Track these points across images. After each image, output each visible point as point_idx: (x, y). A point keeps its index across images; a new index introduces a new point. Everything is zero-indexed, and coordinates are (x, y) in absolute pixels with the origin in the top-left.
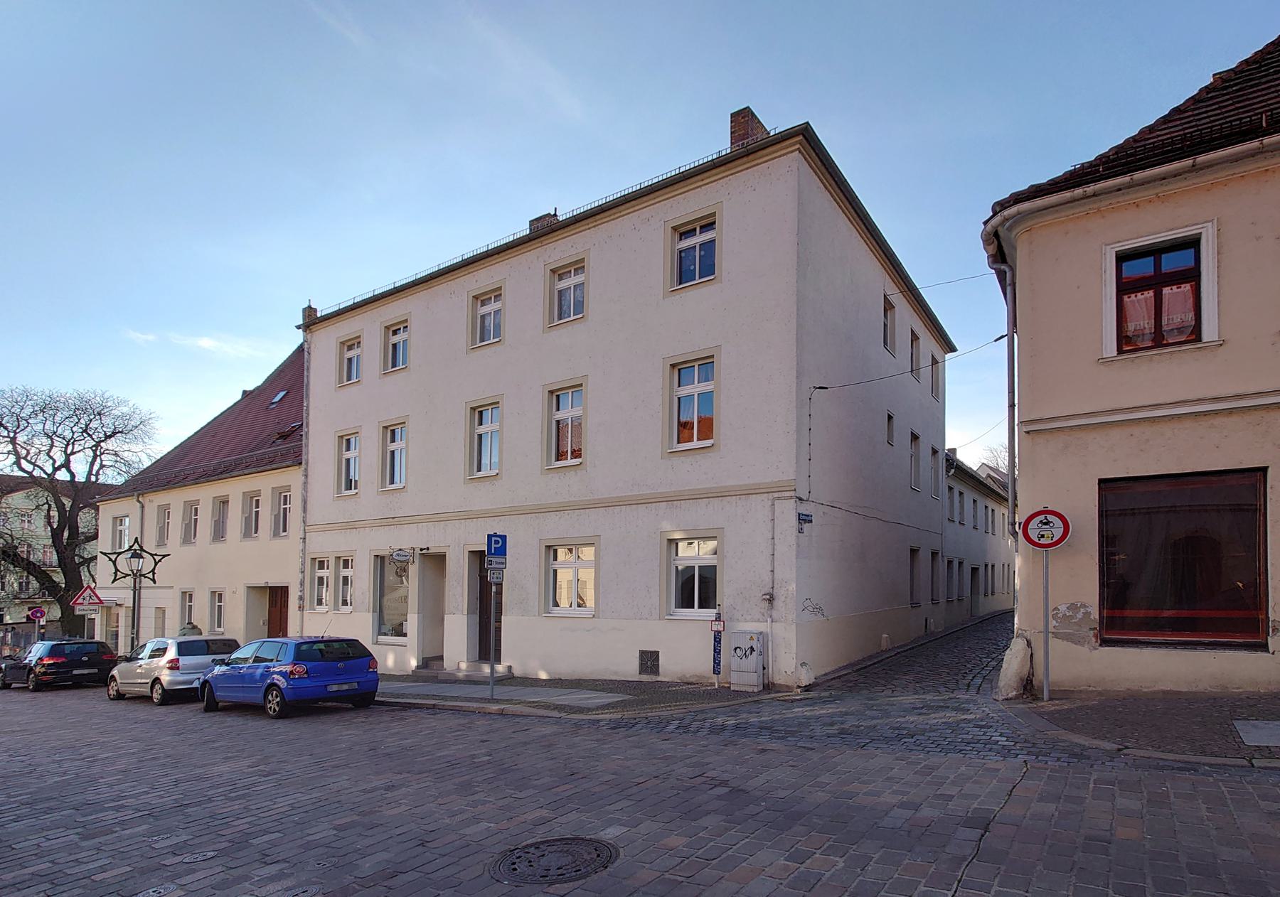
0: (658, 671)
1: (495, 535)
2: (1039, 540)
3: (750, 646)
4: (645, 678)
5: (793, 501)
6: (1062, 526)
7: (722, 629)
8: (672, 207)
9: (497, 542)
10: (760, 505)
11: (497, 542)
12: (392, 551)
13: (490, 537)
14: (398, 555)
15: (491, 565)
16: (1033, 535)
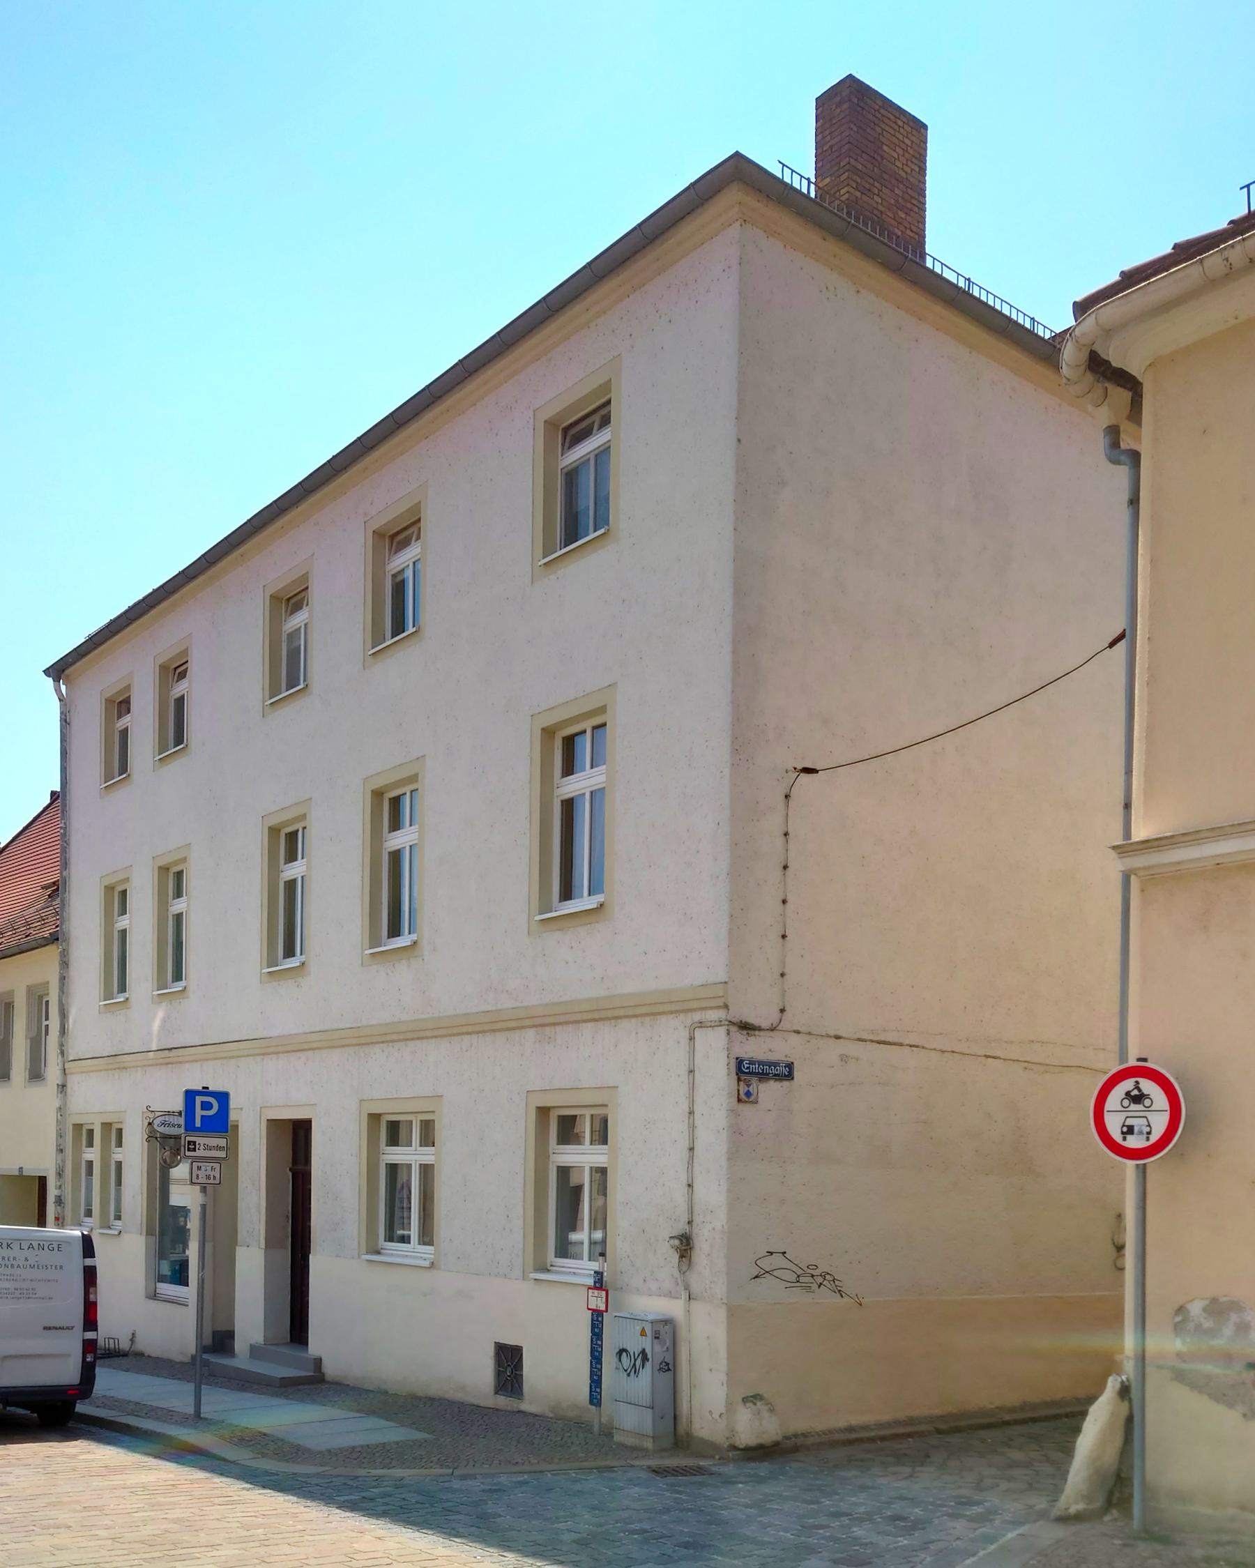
0: (522, 1391)
1: (205, 1091)
2: (1124, 1139)
3: (640, 1350)
4: (503, 1402)
5: (722, 1031)
6: (1106, 1114)
7: (603, 1307)
8: (545, 375)
9: (207, 1106)
10: (672, 1031)
11: (207, 1106)
12: (151, 1115)
13: (190, 1095)
14: (163, 1124)
15: (194, 1150)
16: (1114, 1125)
